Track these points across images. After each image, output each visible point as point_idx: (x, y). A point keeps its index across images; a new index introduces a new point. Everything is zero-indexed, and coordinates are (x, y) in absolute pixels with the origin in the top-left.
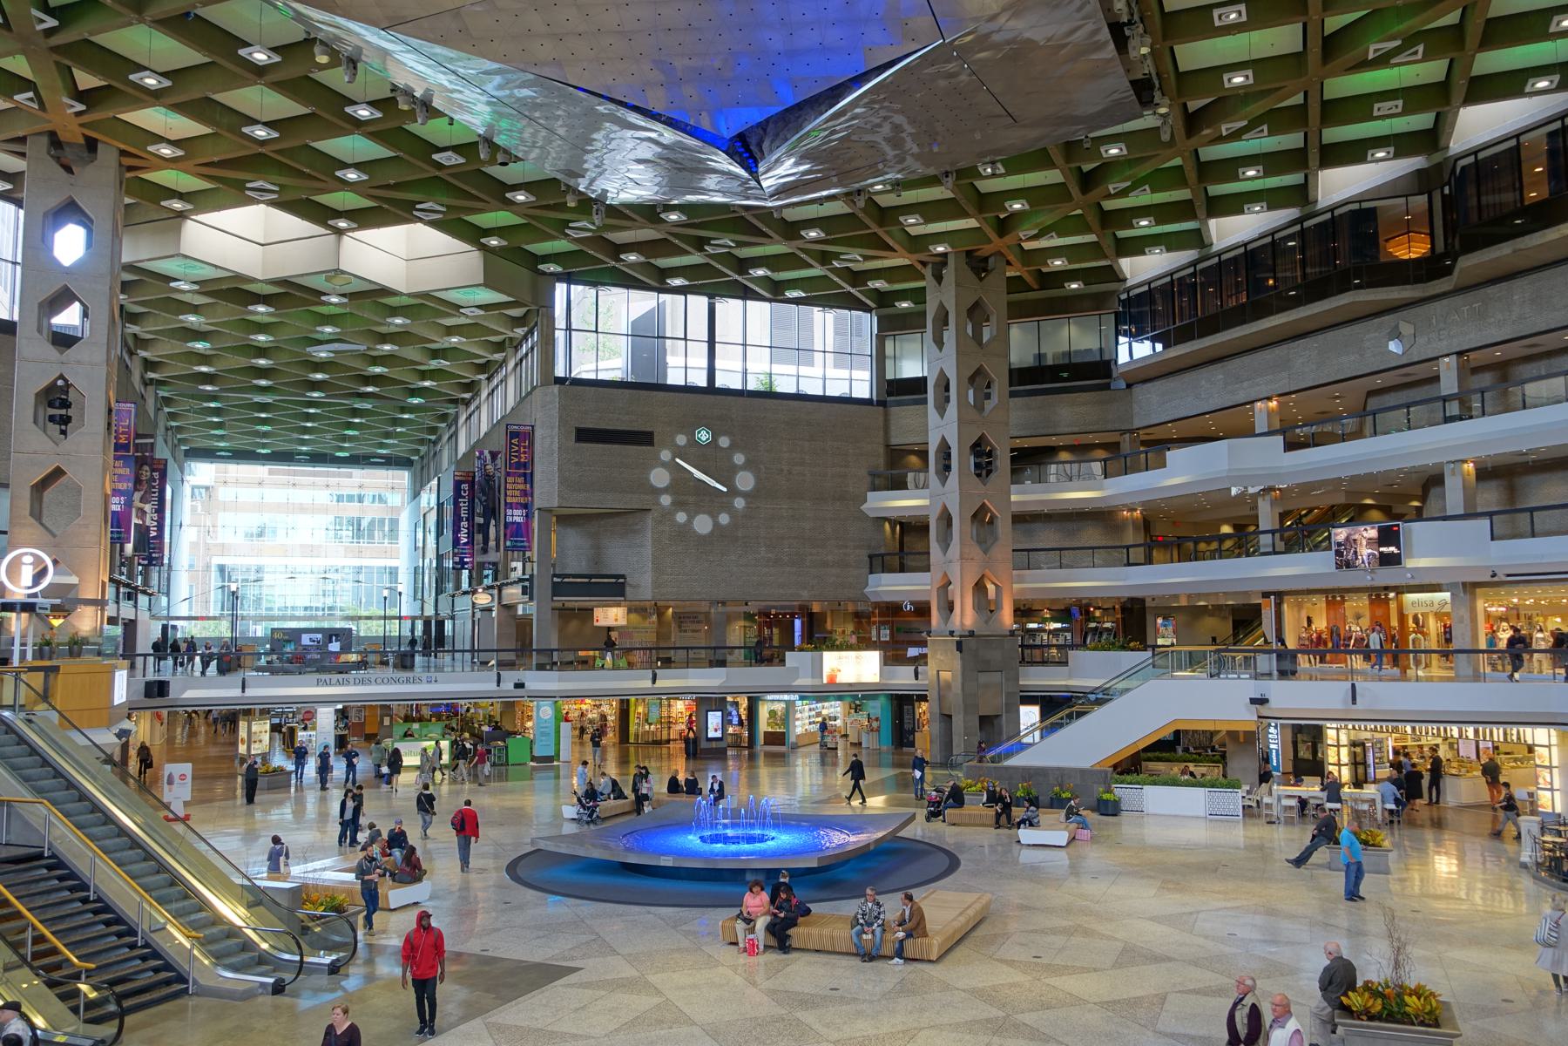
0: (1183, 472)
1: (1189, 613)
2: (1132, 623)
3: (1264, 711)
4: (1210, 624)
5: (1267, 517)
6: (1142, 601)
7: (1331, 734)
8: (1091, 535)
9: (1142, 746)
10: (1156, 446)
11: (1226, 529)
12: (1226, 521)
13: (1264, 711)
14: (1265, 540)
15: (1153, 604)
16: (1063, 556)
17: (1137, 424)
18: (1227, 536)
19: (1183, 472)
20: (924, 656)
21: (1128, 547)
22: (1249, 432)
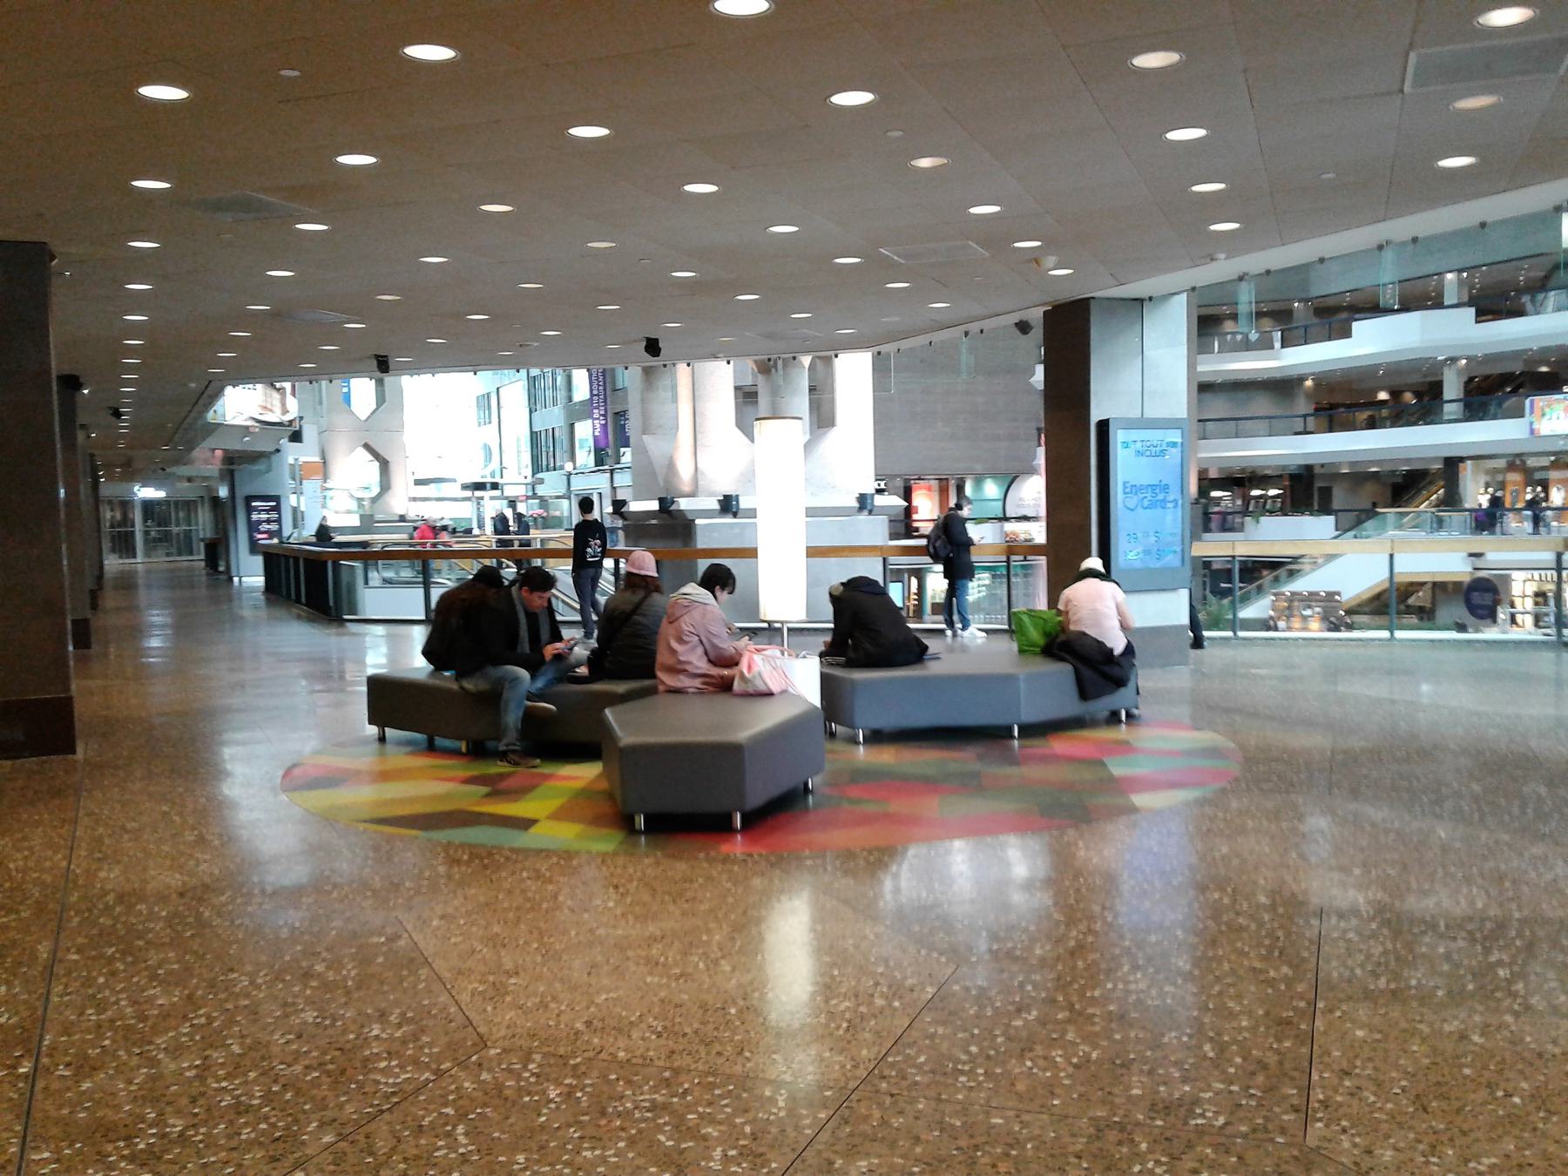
0: (1372, 341)
1: (1360, 477)
2: (1304, 490)
3: (1480, 563)
4: (1370, 488)
5: (1452, 388)
6: (1309, 468)
7: (1516, 589)
8: (1262, 405)
9: (1365, 597)
10: (1333, 317)
11: (1383, 396)
12: (1382, 389)
13: (1480, 563)
14: (1449, 409)
15: (1322, 471)
16: (1235, 426)
17: (1316, 291)
18: (1384, 402)
19: (1372, 341)
20: (1206, 519)
21: (1305, 416)
22: (1438, 304)
